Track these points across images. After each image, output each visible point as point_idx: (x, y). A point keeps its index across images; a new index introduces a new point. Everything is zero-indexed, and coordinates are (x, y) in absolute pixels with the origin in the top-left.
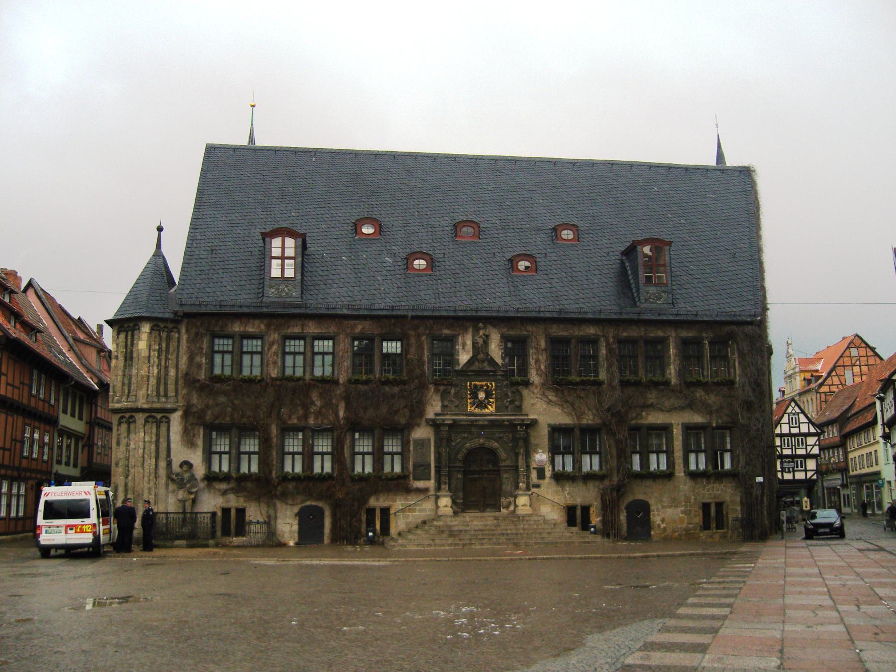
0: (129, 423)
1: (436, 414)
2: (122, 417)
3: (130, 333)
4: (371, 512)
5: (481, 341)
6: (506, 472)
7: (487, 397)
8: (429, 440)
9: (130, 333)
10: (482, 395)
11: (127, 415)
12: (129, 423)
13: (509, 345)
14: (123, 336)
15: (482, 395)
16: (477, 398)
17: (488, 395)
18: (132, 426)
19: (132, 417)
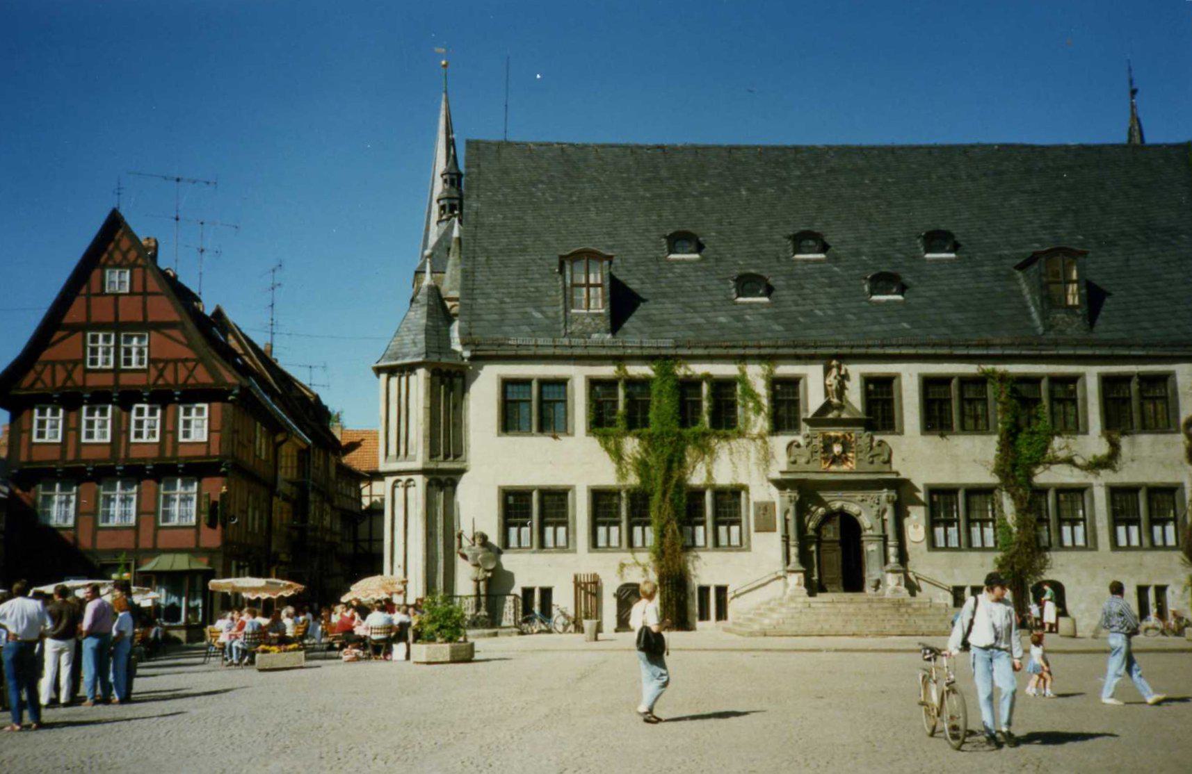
0: (406, 487)
1: (782, 472)
2: (398, 481)
3: (404, 379)
4: (704, 590)
5: (835, 383)
6: (871, 542)
7: (844, 452)
8: (774, 503)
9: (404, 379)
10: (837, 449)
11: (404, 478)
12: (406, 487)
13: (871, 387)
14: (394, 381)
15: (837, 449)
16: (832, 451)
17: (846, 445)
18: (411, 490)
19: (410, 480)
